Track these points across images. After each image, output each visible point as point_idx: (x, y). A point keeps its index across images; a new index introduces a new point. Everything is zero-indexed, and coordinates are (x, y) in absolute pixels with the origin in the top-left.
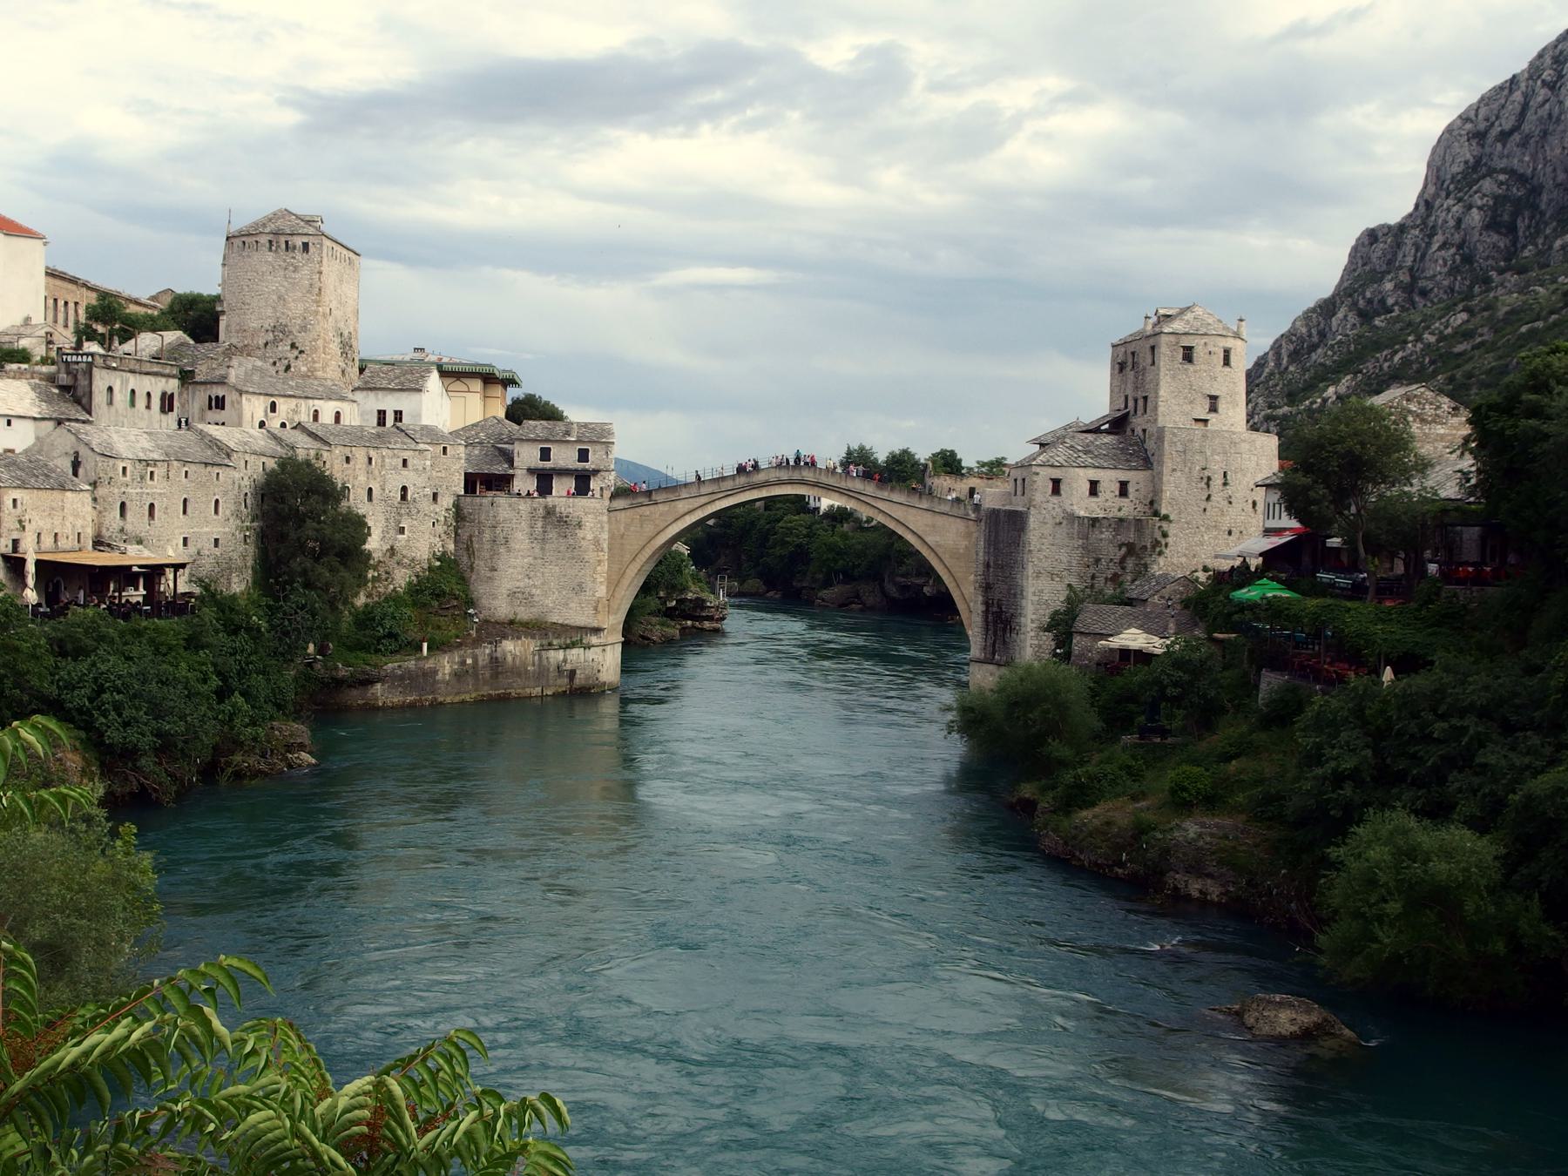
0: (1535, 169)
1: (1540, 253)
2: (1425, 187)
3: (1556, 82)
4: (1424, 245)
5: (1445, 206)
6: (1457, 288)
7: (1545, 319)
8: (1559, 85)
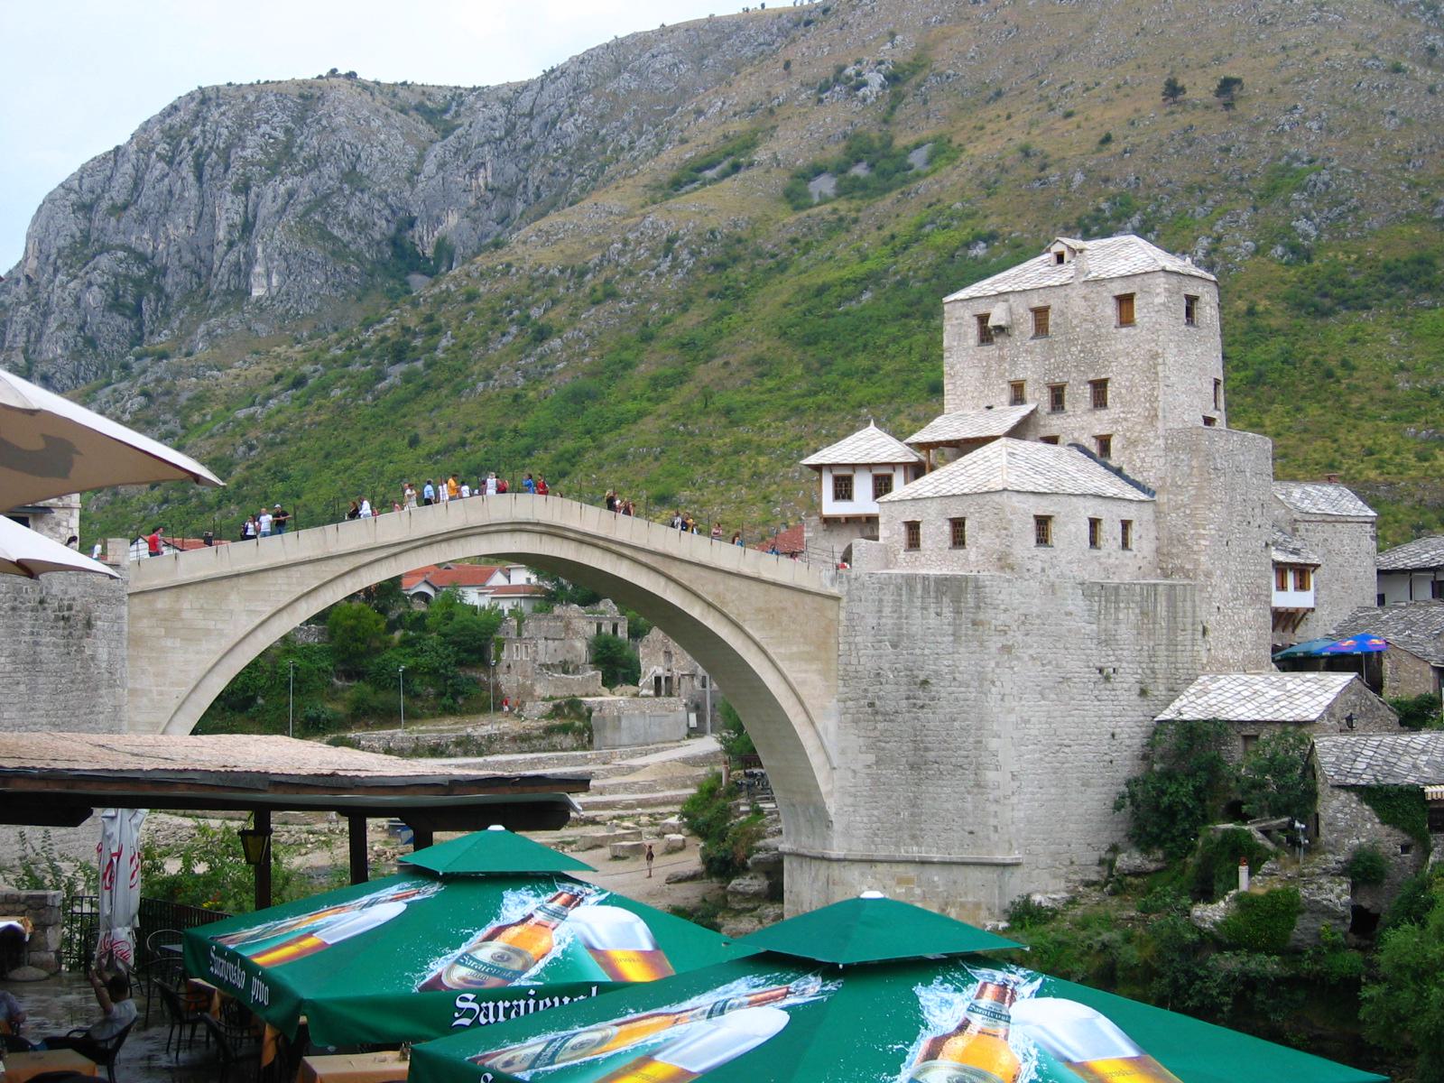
0: (155, 248)
1: (179, 339)
2: (26, 259)
3: (173, 157)
4: (38, 325)
5: (57, 282)
6: (81, 374)
7: (263, 405)
8: (178, 159)
